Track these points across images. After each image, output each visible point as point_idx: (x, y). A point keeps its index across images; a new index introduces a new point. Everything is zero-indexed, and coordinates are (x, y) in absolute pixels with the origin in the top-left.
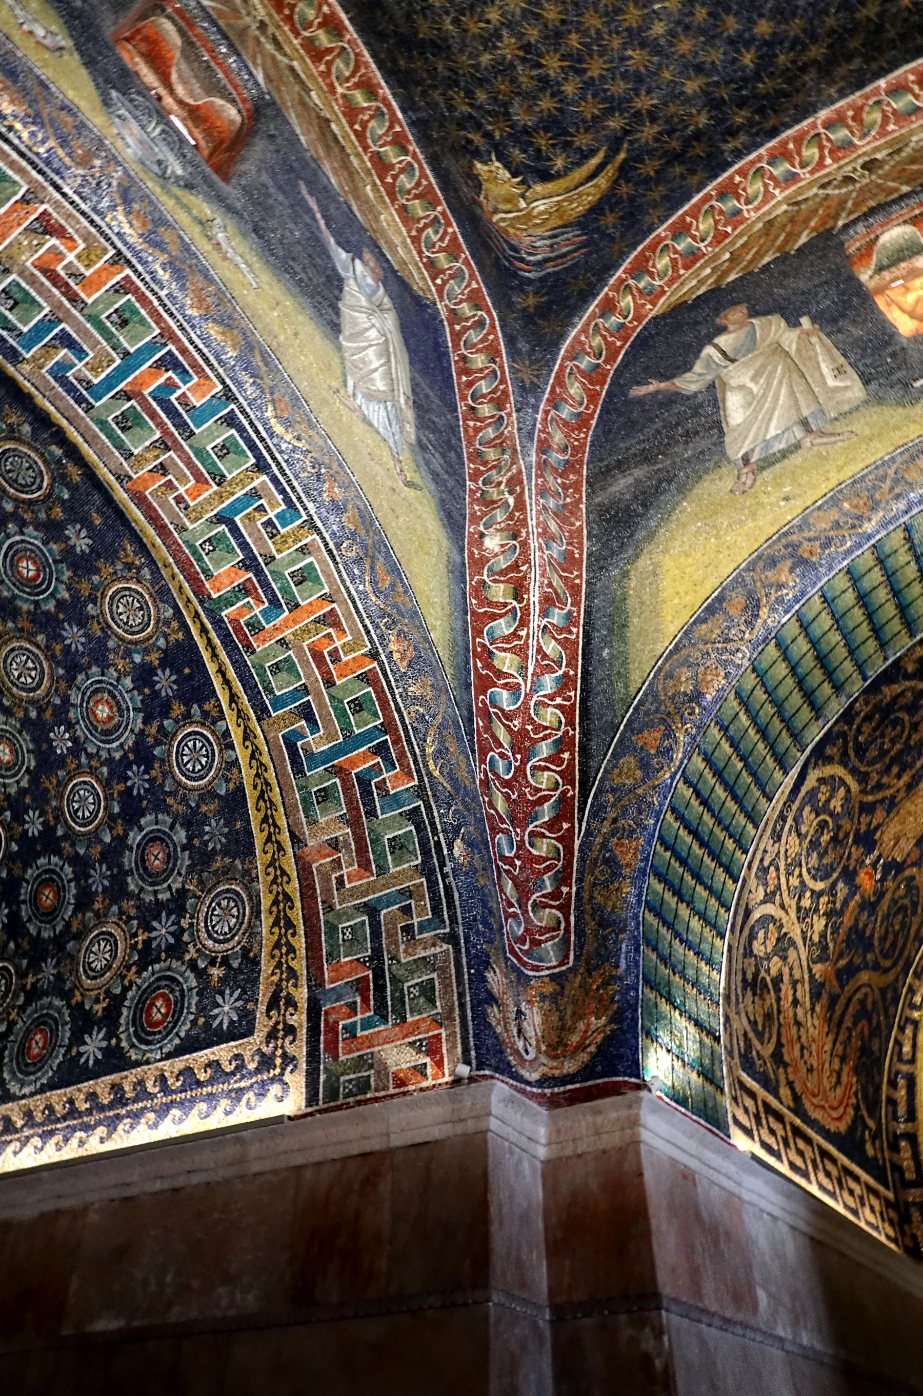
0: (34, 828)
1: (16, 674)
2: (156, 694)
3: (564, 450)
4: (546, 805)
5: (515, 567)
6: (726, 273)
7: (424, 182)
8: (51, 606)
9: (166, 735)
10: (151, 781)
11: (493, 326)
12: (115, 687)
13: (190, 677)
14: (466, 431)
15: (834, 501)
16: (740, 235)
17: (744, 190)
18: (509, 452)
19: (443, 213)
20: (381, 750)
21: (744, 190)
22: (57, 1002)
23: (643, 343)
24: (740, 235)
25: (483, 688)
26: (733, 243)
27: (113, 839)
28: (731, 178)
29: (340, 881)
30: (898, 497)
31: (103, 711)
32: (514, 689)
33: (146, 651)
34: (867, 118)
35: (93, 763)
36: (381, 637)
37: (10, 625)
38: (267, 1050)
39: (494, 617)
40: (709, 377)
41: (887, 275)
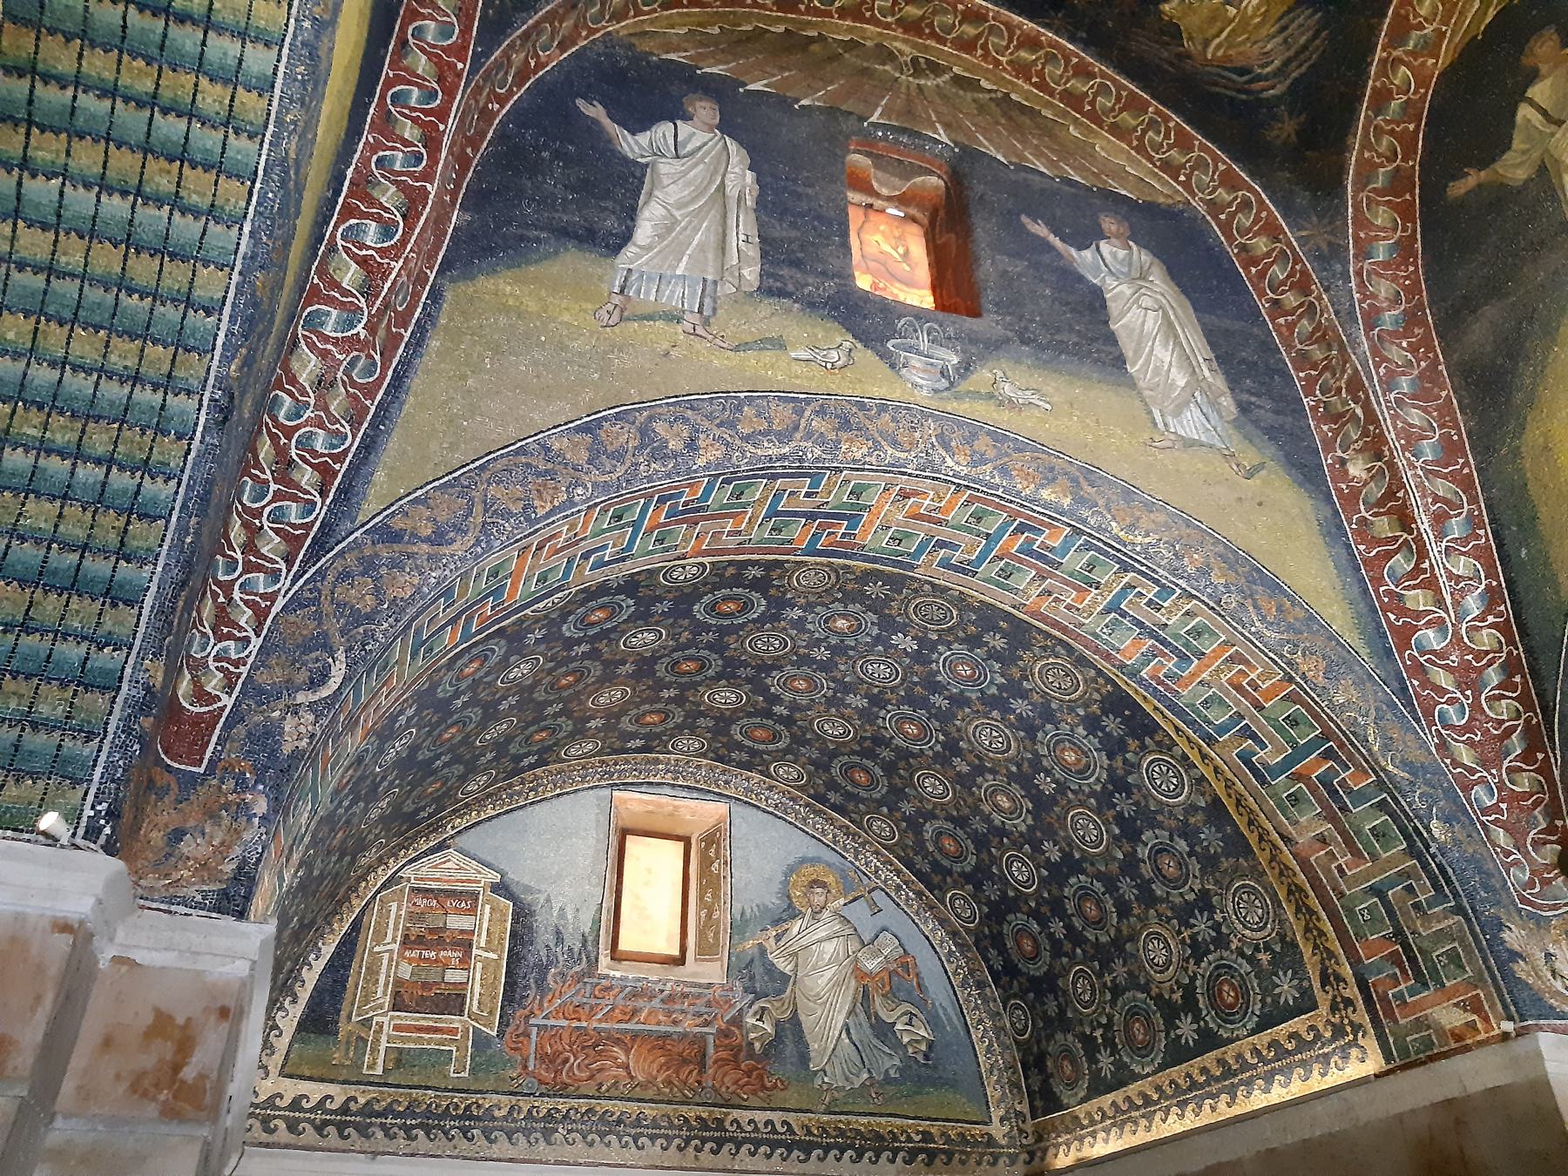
0: (1055, 856)
2: (1109, 735)
3: (1396, 301)
4: (1514, 736)
5: (1390, 495)
7: (1124, 94)
9: (1132, 765)
10: (1137, 804)
11: (1261, 202)
13: (1132, 716)
14: (1280, 334)
18: (1335, 346)
20: (1329, 755)
22: (1141, 996)
25: (1404, 644)
29: (1339, 868)
31: (1070, 757)
32: (1439, 624)
35: (1081, 797)
36: (1289, 663)
37: (967, 710)
38: (1336, 1020)
39: (1389, 555)
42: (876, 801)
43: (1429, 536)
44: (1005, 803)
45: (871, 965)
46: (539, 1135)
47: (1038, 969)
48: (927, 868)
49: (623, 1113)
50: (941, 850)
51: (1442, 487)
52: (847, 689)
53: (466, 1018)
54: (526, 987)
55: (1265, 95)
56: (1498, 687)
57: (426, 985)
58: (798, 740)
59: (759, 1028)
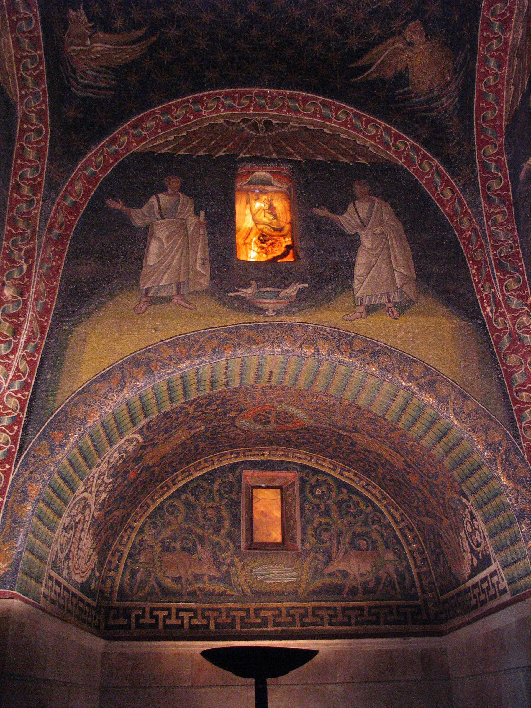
3: (60, 227)
5: (16, 316)
6: (179, 147)
15: (173, 343)
16: (196, 124)
17: (207, 103)
19: (40, 56)
21: (207, 103)
23: (123, 167)
24: (196, 124)
26: (190, 127)
28: (202, 97)
30: (199, 356)
34: (276, 102)
40: (148, 221)
41: (252, 187)
43: (21, 346)
51: (36, 326)
55: (73, 89)
56: (5, 426)
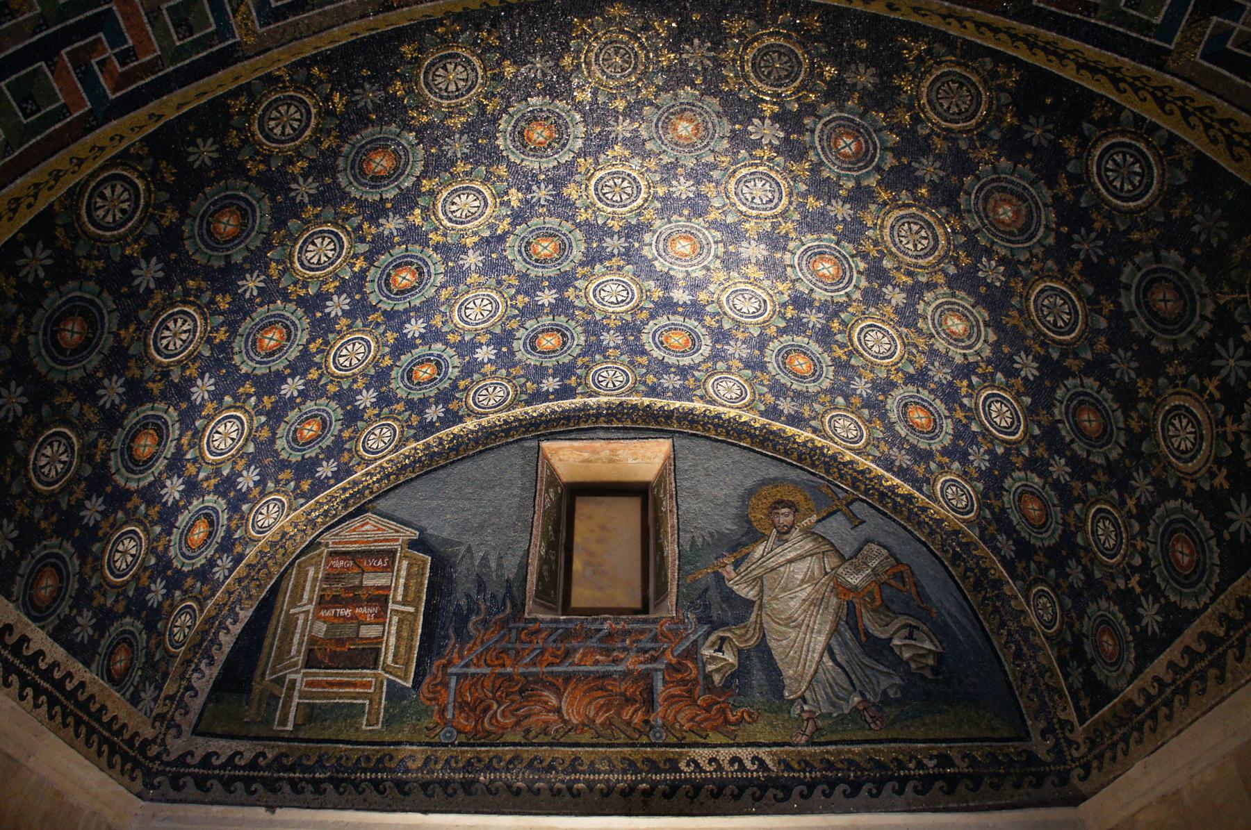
1: (910, 246)
8: (890, 161)
12: (998, 180)
22: (1172, 504)
27: (1109, 319)
31: (1006, 213)
33: (998, 120)
35: (1036, 267)
37: (873, 207)
42: (825, 391)
44: (957, 325)
45: (855, 580)
46: (456, 786)
47: (1049, 538)
48: (903, 459)
49: (554, 759)
50: (912, 428)
52: (734, 233)
53: (380, 671)
54: (447, 637)
57: (340, 642)
58: (721, 336)
59: (720, 659)
